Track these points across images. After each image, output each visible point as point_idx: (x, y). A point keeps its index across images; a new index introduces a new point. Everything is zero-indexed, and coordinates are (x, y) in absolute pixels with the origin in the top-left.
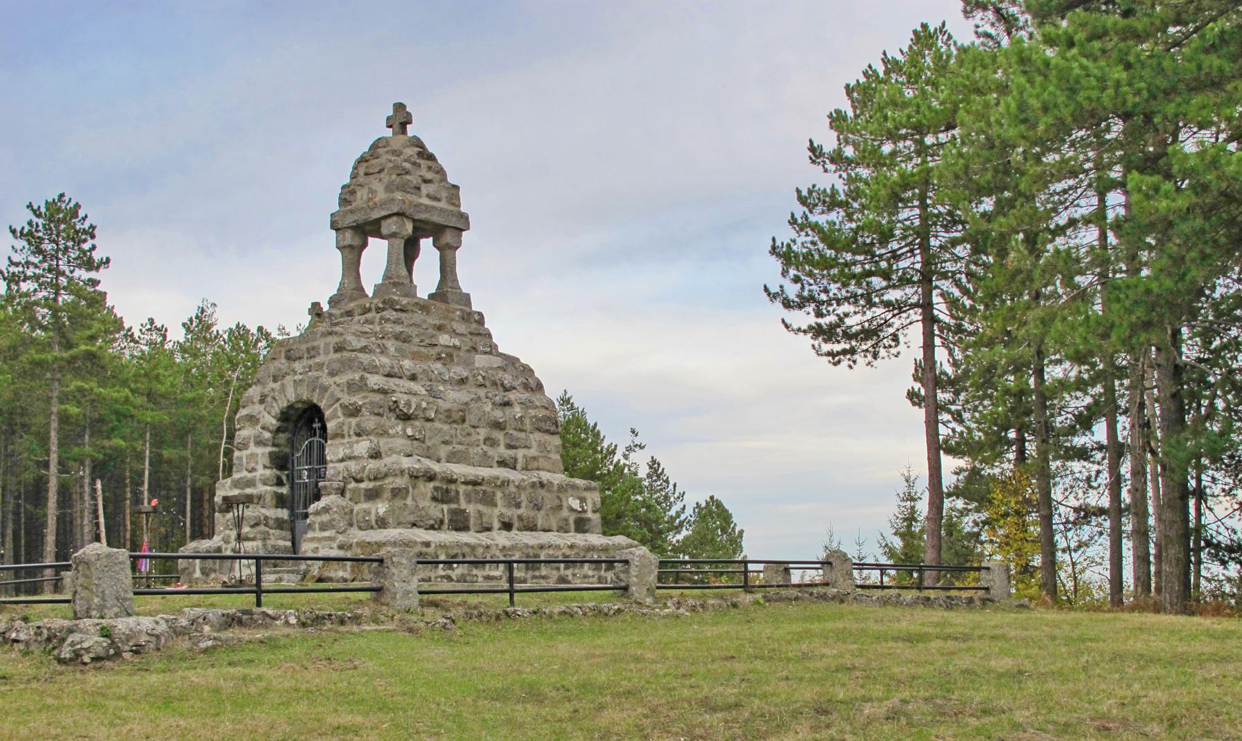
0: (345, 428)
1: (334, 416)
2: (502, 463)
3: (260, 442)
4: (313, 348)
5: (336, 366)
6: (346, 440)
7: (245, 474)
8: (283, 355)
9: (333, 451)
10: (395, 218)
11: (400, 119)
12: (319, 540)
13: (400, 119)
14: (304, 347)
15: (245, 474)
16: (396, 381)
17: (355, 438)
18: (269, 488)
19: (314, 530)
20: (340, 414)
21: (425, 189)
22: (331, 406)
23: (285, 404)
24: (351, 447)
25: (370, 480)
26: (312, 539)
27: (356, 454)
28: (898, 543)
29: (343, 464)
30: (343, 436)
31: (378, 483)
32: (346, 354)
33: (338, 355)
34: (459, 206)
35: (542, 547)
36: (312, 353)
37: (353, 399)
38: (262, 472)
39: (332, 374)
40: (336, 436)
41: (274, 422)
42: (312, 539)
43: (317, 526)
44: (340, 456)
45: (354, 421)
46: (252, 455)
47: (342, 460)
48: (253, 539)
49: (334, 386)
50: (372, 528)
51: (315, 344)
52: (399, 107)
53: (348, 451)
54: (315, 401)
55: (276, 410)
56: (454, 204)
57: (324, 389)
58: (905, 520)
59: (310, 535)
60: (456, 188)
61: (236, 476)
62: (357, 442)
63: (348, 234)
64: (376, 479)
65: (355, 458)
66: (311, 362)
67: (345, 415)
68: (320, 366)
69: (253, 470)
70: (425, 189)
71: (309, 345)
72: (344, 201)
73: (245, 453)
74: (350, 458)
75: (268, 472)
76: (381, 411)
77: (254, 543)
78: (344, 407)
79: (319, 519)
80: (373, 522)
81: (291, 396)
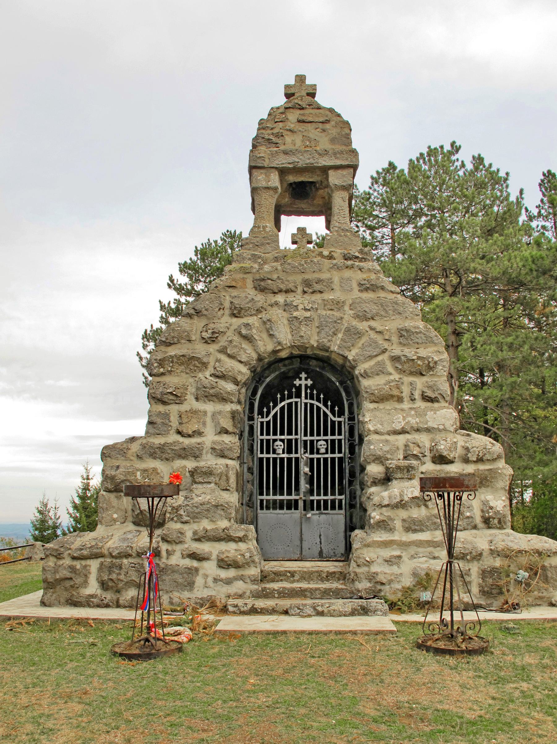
0: (406, 390)
1: (381, 371)
3: (206, 395)
4: (319, 281)
5: (373, 309)
6: (406, 405)
7: (173, 437)
8: (250, 283)
9: (372, 417)
12: (404, 545)
14: (299, 278)
15: (173, 437)
17: (420, 404)
18: (230, 462)
19: (391, 530)
20: (390, 369)
22: (371, 357)
23: (270, 347)
24: (421, 414)
25: (466, 460)
26: (386, 544)
27: (431, 424)
28: (77, 501)
29: (401, 439)
30: (400, 400)
31: (482, 467)
32: (382, 294)
33: (370, 295)
36: (317, 287)
37: (423, 352)
38: (210, 437)
39: (364, 317)
40: (381, 399)
41: (244, 372)
42: (386, 544)
43: (398, 524)
44: (398, 427)
45: (420, 383)
46: (194, 412)
47: (403, 432)
48: (241, 540)
49: (372, 334)
50: (475, 527)
51: (325, 276)
53: (414, 421)
54: (334, 348)
55: (248, 353)
57: (354, 334)
58: (83, 489)
59: (380, 536)
62: (435, 410)
64: (480, 460)
65: (428, 430)
66: (317, 297)
67: (402, 371)
68: (338, 305)
69: (199, 433)
71: (307, 276)
73: (174, 409)
74: (418, 430)
75: (227, 439)
77: (242, 546)
78: (395, 359)
79: (403, 514)
80: (478, 520)
81: (285, 336)
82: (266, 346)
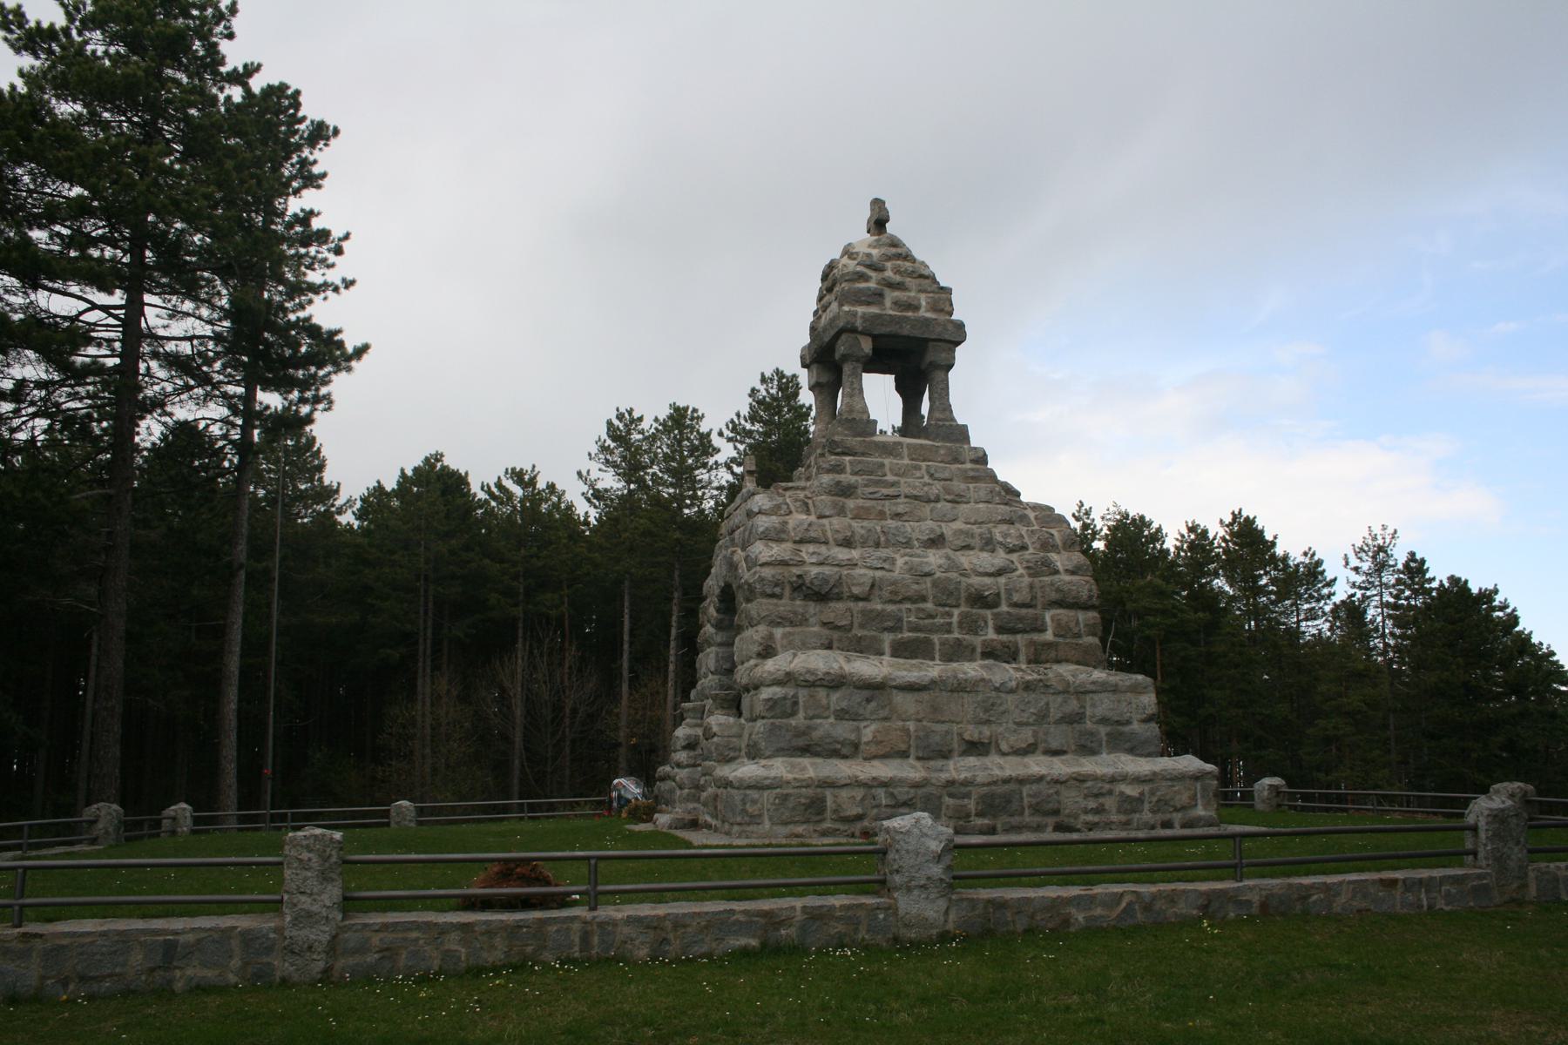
2: (990, 653)
10: (844, 337)
11: (879, 223)
13: (879, 223)
16: (811, 548)
21: (891, 296)
34: (951, 314)
35: (1021, 781)
52: (878, 204)
56: (942, 310)
60: (948, 291)
61: (699, 686)
63: (814, 367)
70: (891, 296)
72: (813, 329)
76: (777, 590)
82: (717, 591)
